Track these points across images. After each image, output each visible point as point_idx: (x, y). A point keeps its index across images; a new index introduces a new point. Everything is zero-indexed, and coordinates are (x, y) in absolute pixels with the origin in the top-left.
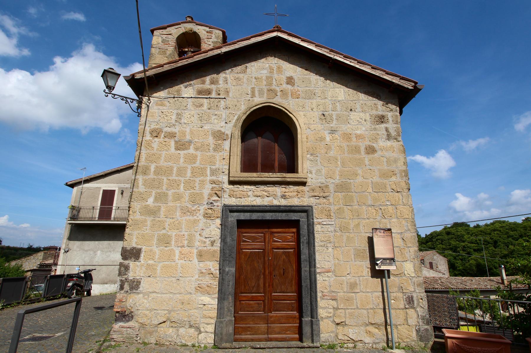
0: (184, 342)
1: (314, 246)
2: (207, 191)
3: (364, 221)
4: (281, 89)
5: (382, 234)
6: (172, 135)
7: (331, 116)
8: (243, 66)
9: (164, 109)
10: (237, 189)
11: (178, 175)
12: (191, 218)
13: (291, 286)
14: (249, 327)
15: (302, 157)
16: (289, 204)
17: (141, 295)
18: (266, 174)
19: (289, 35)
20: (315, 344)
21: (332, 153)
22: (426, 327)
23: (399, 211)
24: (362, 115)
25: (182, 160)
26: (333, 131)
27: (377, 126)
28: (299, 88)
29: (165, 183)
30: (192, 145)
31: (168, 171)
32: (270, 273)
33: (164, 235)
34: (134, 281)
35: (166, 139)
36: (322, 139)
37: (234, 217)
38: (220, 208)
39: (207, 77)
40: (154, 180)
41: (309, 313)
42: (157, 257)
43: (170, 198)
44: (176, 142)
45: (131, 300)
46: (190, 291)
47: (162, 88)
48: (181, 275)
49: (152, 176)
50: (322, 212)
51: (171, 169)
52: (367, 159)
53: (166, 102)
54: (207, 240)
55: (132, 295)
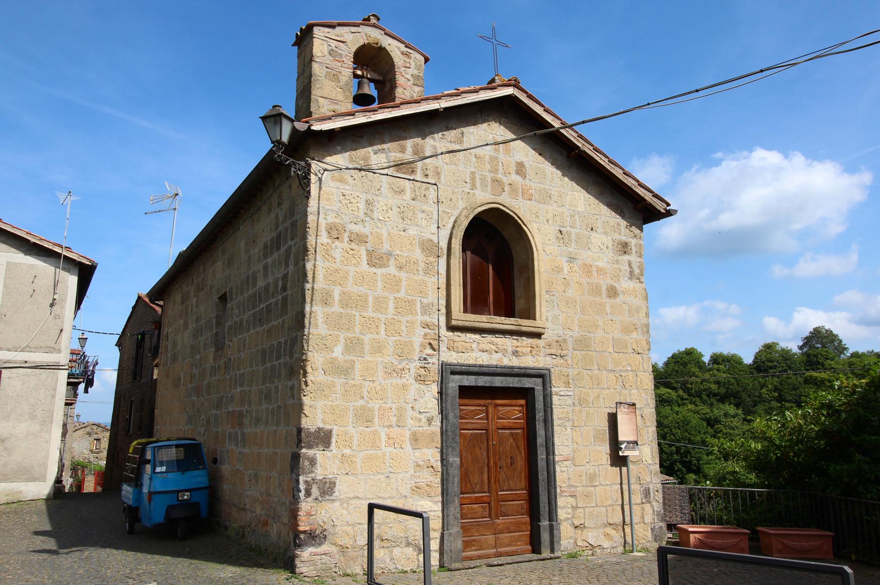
0: (400, 568)
1: (552, 425)
2: (418, 338)
3: (604, 392)
4: (509, 182)
5: (626, 410)
6: (359, 239)
7: (570, 235)
8: (459, 131)
9: (347, 189)
10: (457, 339)
11: (377, 310)
12: (399, 381)
13: (521, 481)
14: (473, 540)
15: (540, 296)
16: (523, 365)
17: (337, 504)
18: (498, 319)
19: (530, 97)
20: (556, 554)
21: (570, 293)
22: (661, 524)
23: (639, 380)
24: (603, 237)
25: (380, 285)
26: (572, 259)
27: (620, 258)
28: (532, 183)
29: (357, 322)
30: (393, 260)
31: (360, 302)
32: (495, 464)
33: (363, 408)
34: (326, 482)
35: (354, 246)
36: (559, 270)
37: (455, 382)
38: (436, 366)
39: (408, 141)
40: (340, 316)
41: (547, 515)
42: (356, 442)
43: (367, 348)
44: (370, 253)
45: (323, 512)
46: (405, 493)
47: (339, 148)
48: (391, 470)
49: (336, 308)
50: (560, 379)
51: (364, 298)
52: (608, 302)
53: (347, 174)
54: (422, 416)
55: (324, 503)
